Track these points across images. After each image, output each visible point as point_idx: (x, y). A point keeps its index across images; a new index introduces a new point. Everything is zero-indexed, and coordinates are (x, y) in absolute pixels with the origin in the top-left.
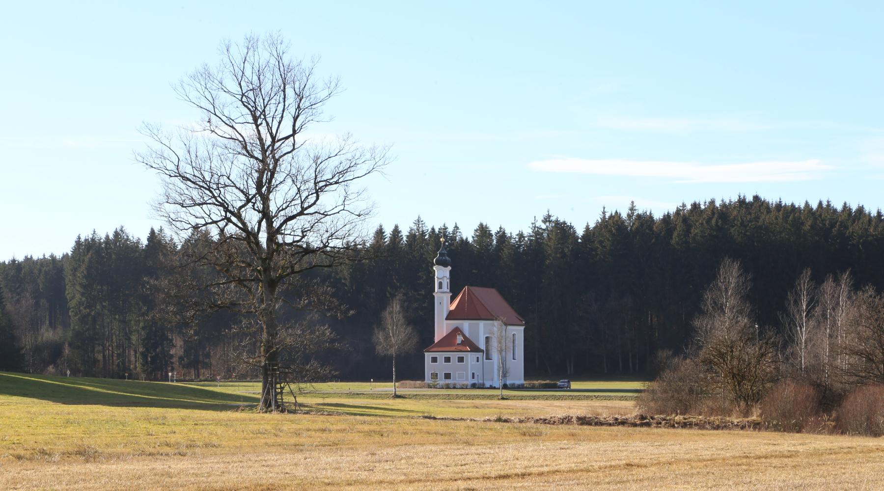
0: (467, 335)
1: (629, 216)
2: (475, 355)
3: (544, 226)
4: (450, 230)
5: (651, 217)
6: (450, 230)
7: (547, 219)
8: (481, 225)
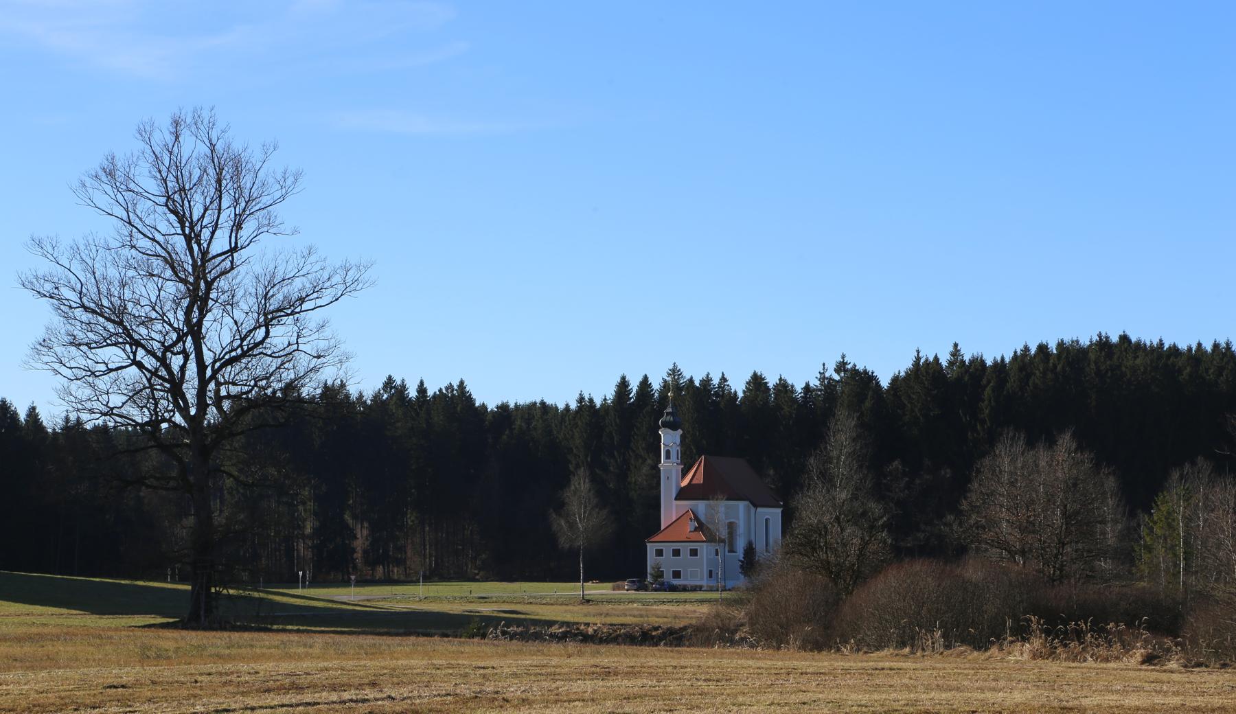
0: (702, 518)
1: (951, 363)
2: (713, 547)
3: (837, 377)
4: (716, 381)
5: (983, 362)
6: (716, 381)
7: (841, 367)
8: (755, 375)
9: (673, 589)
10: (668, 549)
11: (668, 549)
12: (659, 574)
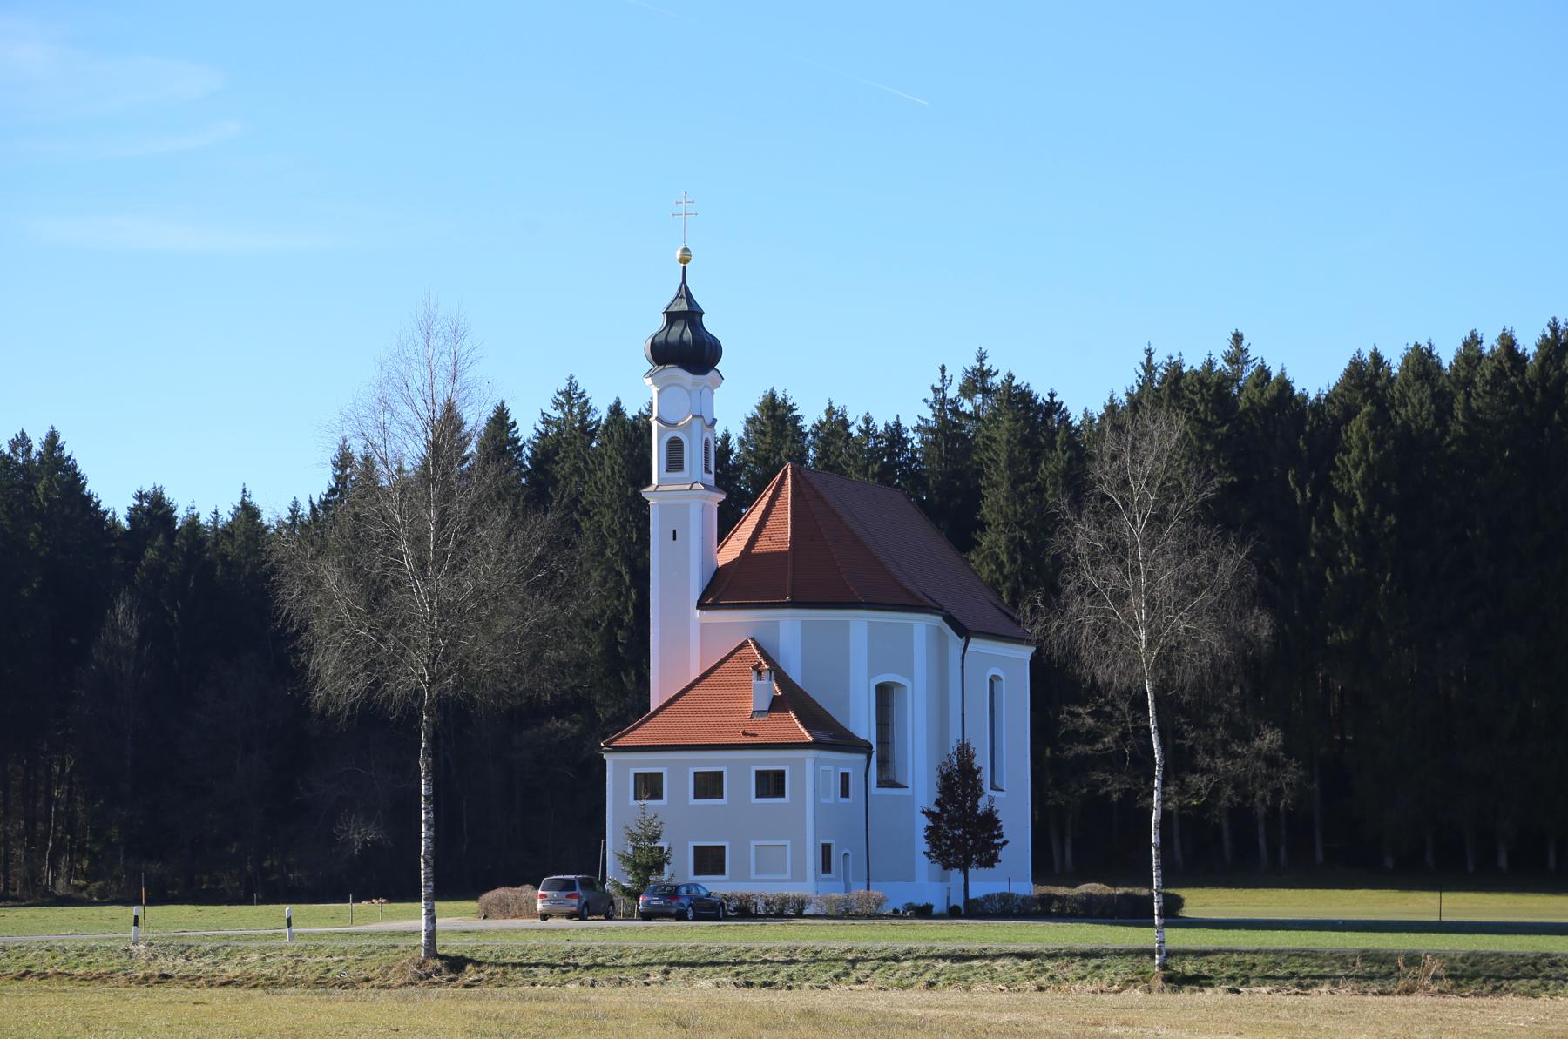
0: (796, 675)
9: (709, 910)
10: (678, 772)
11: (678, 772)
12: (649, 863)
